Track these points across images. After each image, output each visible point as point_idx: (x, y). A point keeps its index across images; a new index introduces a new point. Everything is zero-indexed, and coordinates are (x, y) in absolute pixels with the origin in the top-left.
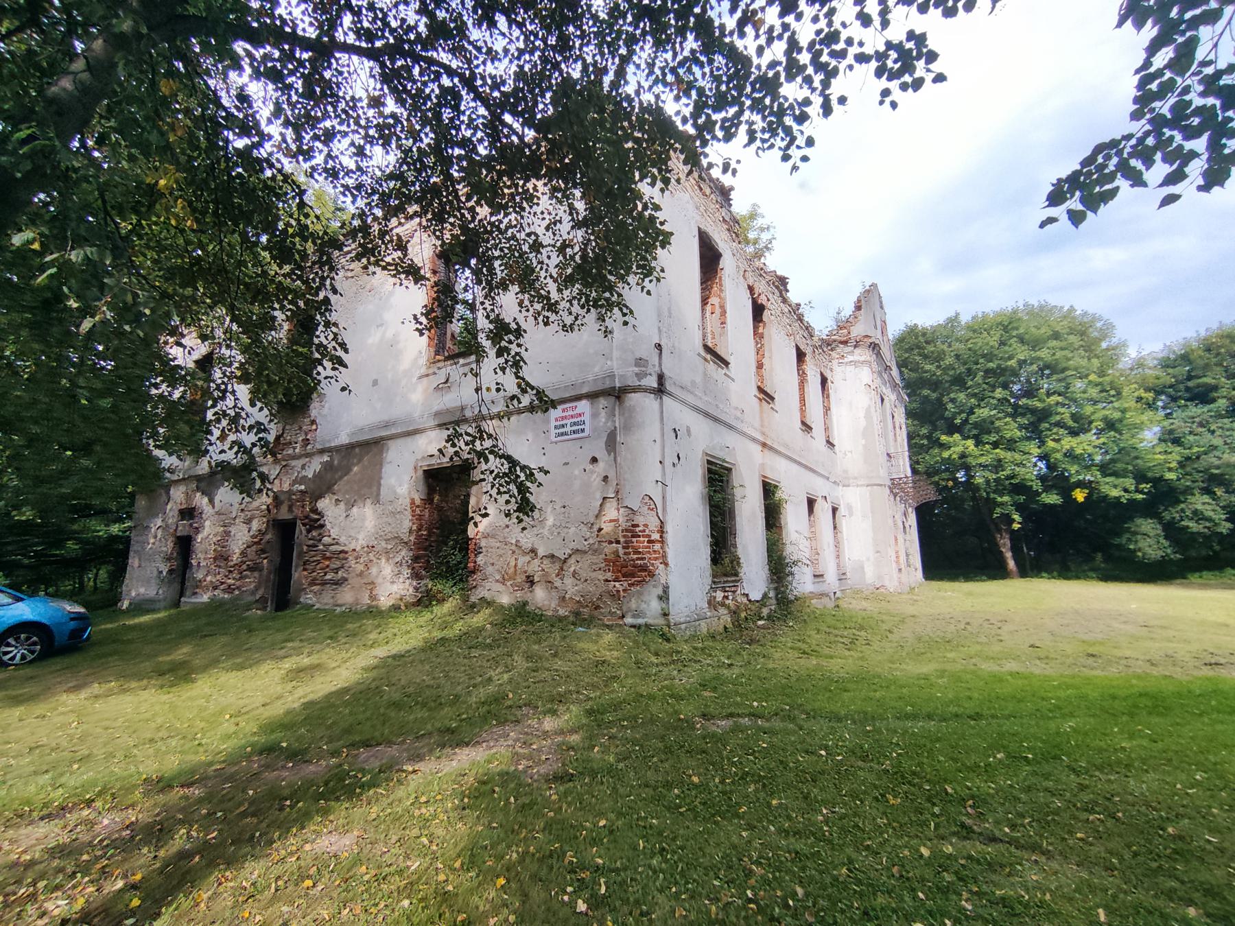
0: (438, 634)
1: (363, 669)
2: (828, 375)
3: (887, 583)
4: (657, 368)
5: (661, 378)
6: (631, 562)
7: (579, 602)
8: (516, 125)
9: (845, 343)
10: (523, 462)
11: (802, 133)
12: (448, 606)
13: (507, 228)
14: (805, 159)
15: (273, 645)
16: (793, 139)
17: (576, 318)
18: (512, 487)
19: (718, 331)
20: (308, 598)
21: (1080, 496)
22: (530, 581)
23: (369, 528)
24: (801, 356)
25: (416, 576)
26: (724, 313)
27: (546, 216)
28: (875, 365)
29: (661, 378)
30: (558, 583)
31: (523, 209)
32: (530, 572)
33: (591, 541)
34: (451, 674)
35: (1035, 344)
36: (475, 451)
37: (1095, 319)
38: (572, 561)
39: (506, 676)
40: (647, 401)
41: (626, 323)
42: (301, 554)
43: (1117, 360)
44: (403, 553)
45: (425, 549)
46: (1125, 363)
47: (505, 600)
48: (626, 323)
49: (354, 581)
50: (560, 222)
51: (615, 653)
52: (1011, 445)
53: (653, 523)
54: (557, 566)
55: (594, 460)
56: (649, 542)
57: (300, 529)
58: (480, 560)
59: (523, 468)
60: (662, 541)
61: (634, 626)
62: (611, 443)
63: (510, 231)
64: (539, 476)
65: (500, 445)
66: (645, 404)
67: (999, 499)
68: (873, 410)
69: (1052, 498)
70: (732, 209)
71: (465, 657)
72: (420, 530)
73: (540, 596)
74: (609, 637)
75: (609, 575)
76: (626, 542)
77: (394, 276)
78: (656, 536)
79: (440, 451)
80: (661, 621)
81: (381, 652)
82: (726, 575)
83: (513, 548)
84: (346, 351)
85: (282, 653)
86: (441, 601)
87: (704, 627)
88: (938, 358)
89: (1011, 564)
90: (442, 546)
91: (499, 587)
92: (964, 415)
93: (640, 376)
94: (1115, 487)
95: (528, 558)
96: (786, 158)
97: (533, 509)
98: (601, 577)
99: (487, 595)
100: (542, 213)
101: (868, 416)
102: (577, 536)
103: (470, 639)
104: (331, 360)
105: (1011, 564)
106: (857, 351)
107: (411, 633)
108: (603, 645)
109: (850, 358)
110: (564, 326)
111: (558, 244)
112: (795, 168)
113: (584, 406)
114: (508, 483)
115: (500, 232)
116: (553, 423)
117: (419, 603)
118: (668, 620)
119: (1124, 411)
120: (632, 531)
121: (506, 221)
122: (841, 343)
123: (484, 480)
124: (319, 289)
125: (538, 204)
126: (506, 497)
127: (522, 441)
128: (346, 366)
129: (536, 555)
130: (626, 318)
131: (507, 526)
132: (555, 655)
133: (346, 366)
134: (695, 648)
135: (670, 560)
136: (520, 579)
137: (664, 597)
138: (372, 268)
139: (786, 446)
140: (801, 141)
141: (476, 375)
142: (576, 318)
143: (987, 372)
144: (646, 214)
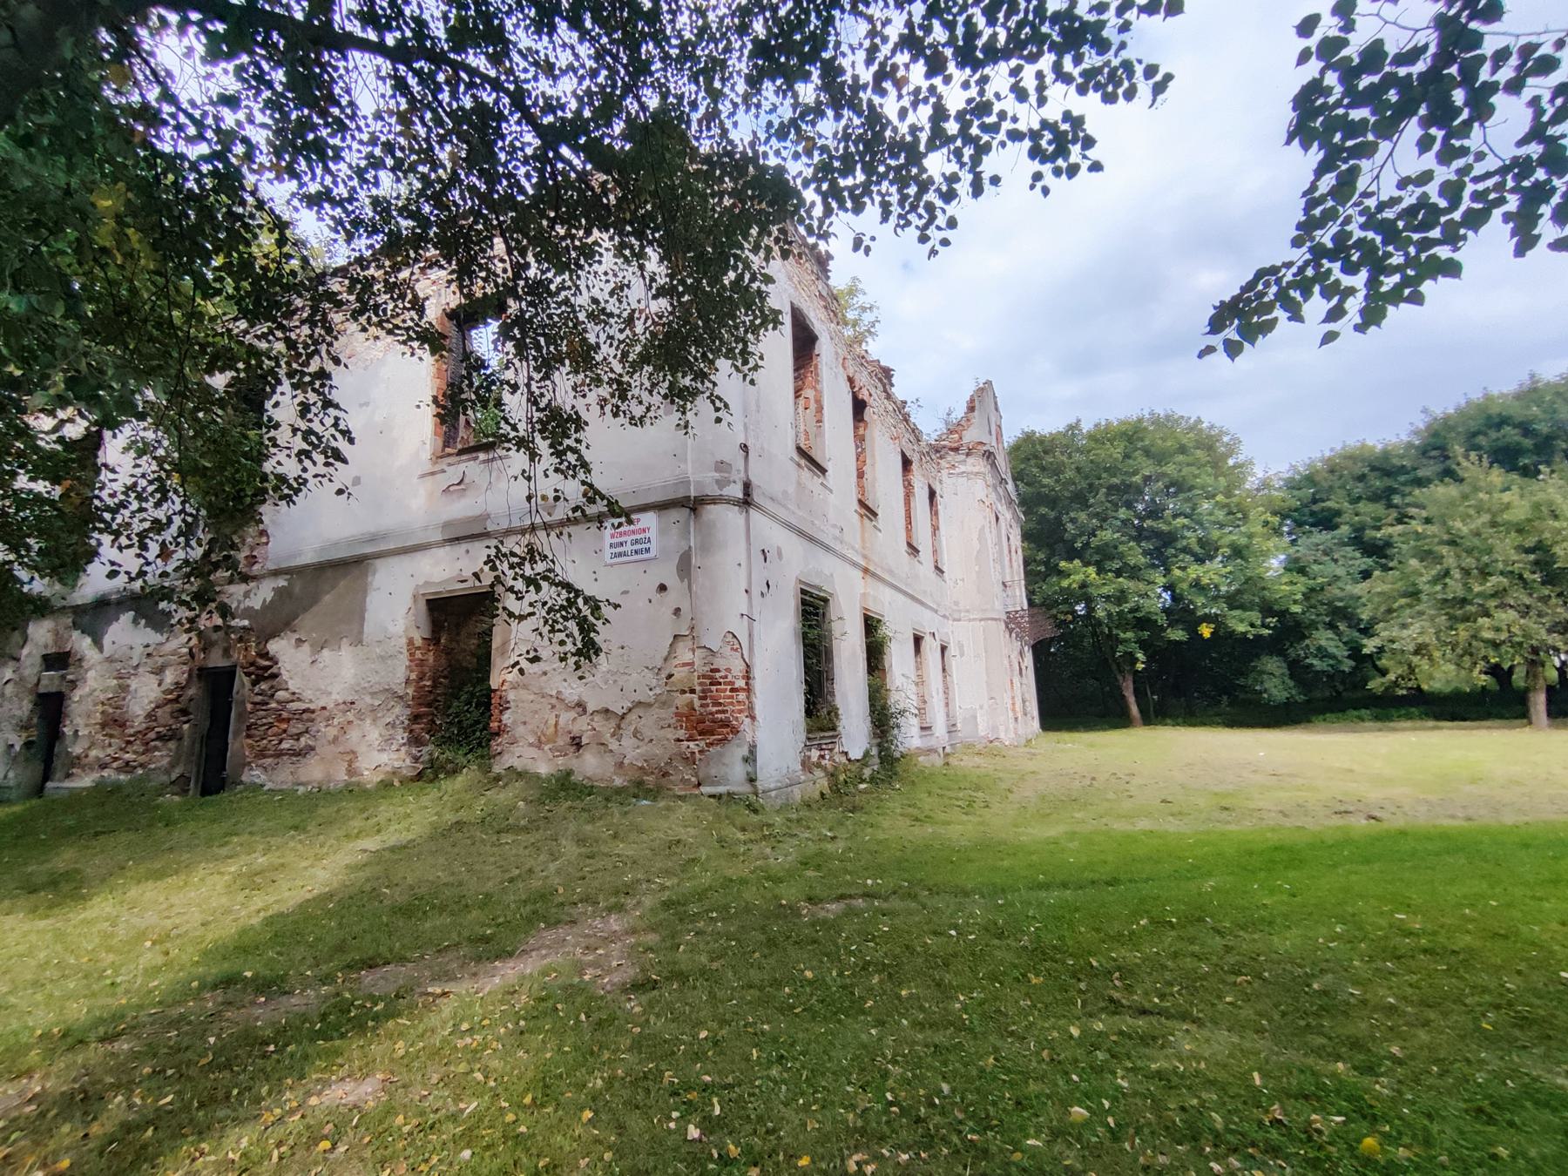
0: (450, 817)
1: (347, 866)
2: (937, 487)
3: (1002, 736)
4: (742, 475)
5: (747, 486)
6: (710, 718)
7: (641, 768)
8: (576, 162)
9: (956, 450)
10: (588, 593)
11: (944, 211)
12: (460, 780)
13: (559, 290)
14: (945, 242)
15: (209, 843)
16: (932, 218)
17: (648, 409)
18: (572, 626)
19: (812, 430)
20: (253, 775)
21: (1206, 631)
22: (576, 743)
23: (348, 679)
24: (906, 463)
25: (415, 741)
26: (820, 409)
27: (610, 277)
28: (990, 480)
29: (747, 486)
30: (613, 745)
31: (581, 267)
32: (576, 733)
33: (658, 691)
34: (477, 867)
35: (1160, 458)
36: (522, 576)
37: (1222, 433)
38: (633, 717)
39: (552, 867)
40: (730, 515)
41: (718, 420)
42: (242, 715)
43: (1244, 480)
44: (397, 710)
45: (429, 705)
46: (1251, 483)
47: (543, 769)
48: (718, 420)
49: (324, 749)
50: (628, 286)
51: (692, 831)
52: (1134, 573)
53: (738, 667)
54: (613, 723)
55: (663, 588)
56: (732, 690)
57: (242, 681)
58: (507, 717)
59: (587, 600)
60: (748, 689)
61: (712, 796)
62: (685, 567)
63: (563, 293)
64: (606, 611)
65: (558, 570)
66: (727, 519)
67: (1122, 635)
68: (987, 530)
69: (1177, 635)
70: (831, 282)
71: (493, 845)
72: (421, 679)
73: (590, 765)
74: (685, 809)
75: (681, 733)
76: (703, 691)
77: (404, 343)
78: (741, 683)
79: (476, 575)
80: (747, 788)
81: (372, 844)
82: (822, 730)
83: (554, 701)
84: (351, 441)
85: (224, 851)
86: (455, 772)
87: (797, 794)
88: (1057, 471)
89: (1134, 710)
90: (455, 695)
91: (533, 752)
92: (1085, 538)
93: (721, 483)
94: (1242, 621)
95: (573, 714)
96: (924, 239)
97: (597, 651)
98: (670, 736)
99: (518, 764)
100: (606, 274)
101: (981, 538)
102: (642, 684)
103: (499, 824)
104: (324, 452)
105: (1134, 710)
106: (970, 460)
107: (413, 818)
108: (676, 822)
109: (963, 468)
110: (632, 418)
111: (625, 314)
112: (933, 252)
113: (648, 520)
114: (566, 619)
115: (551, 295)
116: (608, 540)
117: (420, 776)
118: (755, 787)
119: (1250, 536)
120: (712, 678)
121: (559, 279)
122: (952, 449)
123: (533, 614)
124: (310, 356)
125: (600, 262)
126: (562, 636)
127: (584, 561)
128: (345, 461)
129: (585, 710)
130: (719, 414)
131: (545, 673)
132: (615, 836)
133: (345, 461)
134: (789, 820)
135: (758, 712)
136: (562, 741)
137: (751, 758)
138: (373, 330)
139: (891, 572)
140: (941, 220)
141: (529, 479)
142: (648, 409)
143: (1111, 488)
144: (755, 285)
